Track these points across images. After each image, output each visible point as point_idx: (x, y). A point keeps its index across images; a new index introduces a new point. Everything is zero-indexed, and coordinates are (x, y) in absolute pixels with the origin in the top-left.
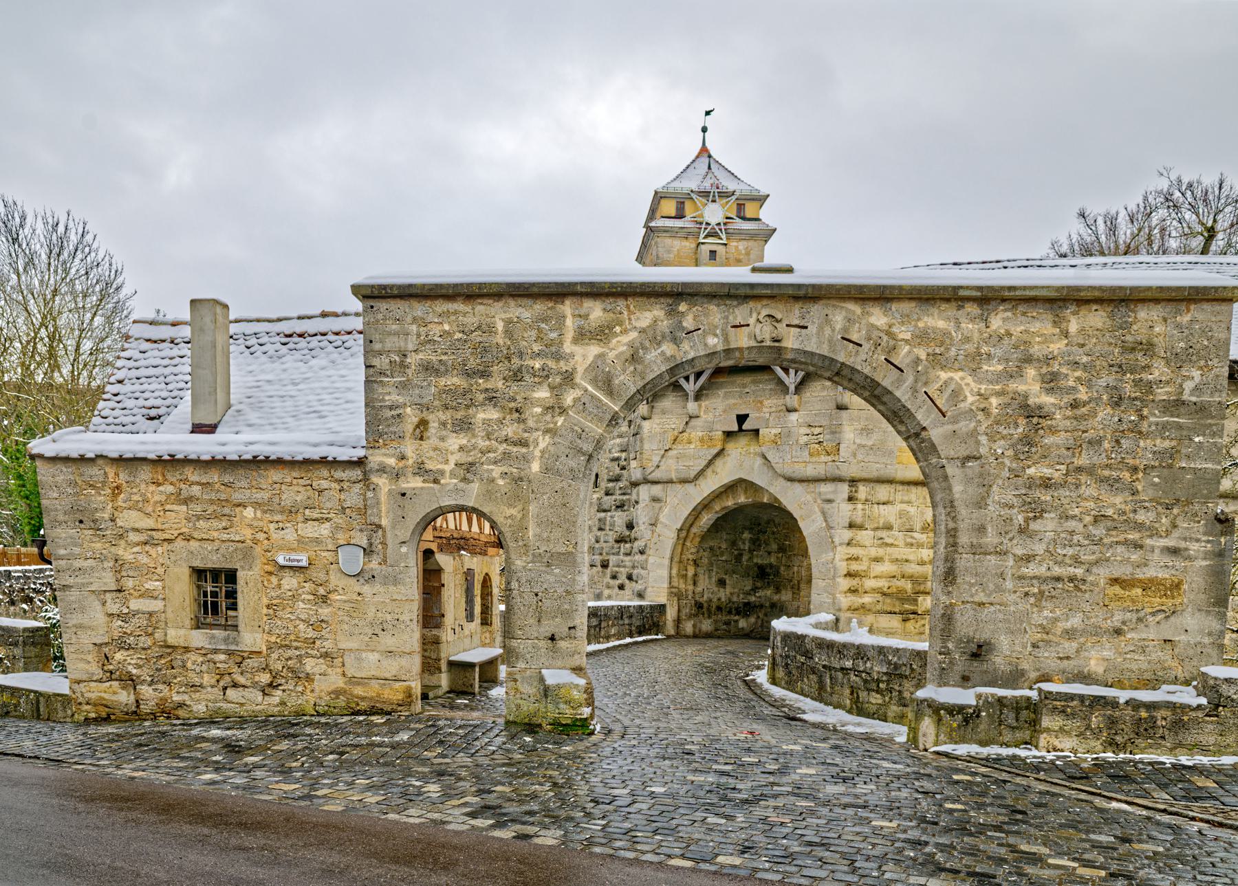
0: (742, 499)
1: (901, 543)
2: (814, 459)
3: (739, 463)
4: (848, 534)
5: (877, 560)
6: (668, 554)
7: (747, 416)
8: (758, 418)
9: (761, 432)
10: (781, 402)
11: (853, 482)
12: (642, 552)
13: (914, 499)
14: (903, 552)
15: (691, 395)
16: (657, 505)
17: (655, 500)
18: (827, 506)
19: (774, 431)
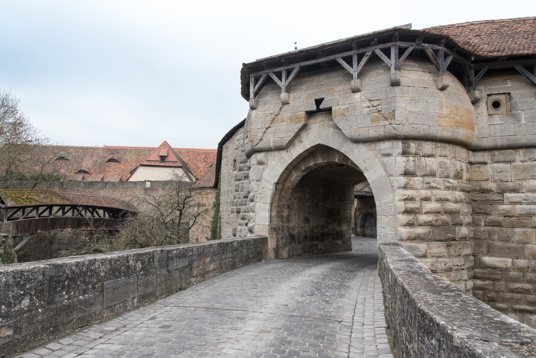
0: (320, 161)
1: (442, 187)
2: (375, 124)
3: (318, 134)
4: (403, 180)
5: (427, 199)
6: (269, 201)
7: (323, 99)
8: (331, 100)
9: (333, 109)
10: (346, 87)
11: (406, 139)
12: (252, 201)
13: (448, 154)
14: (443, 194)
15: (283, 89)
16: (261, 167)
17: (260, 163)
18: (386, 159)
19: (343, 107)
